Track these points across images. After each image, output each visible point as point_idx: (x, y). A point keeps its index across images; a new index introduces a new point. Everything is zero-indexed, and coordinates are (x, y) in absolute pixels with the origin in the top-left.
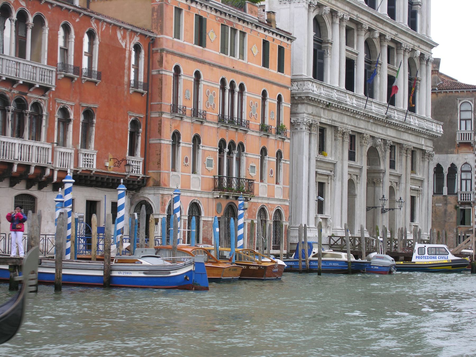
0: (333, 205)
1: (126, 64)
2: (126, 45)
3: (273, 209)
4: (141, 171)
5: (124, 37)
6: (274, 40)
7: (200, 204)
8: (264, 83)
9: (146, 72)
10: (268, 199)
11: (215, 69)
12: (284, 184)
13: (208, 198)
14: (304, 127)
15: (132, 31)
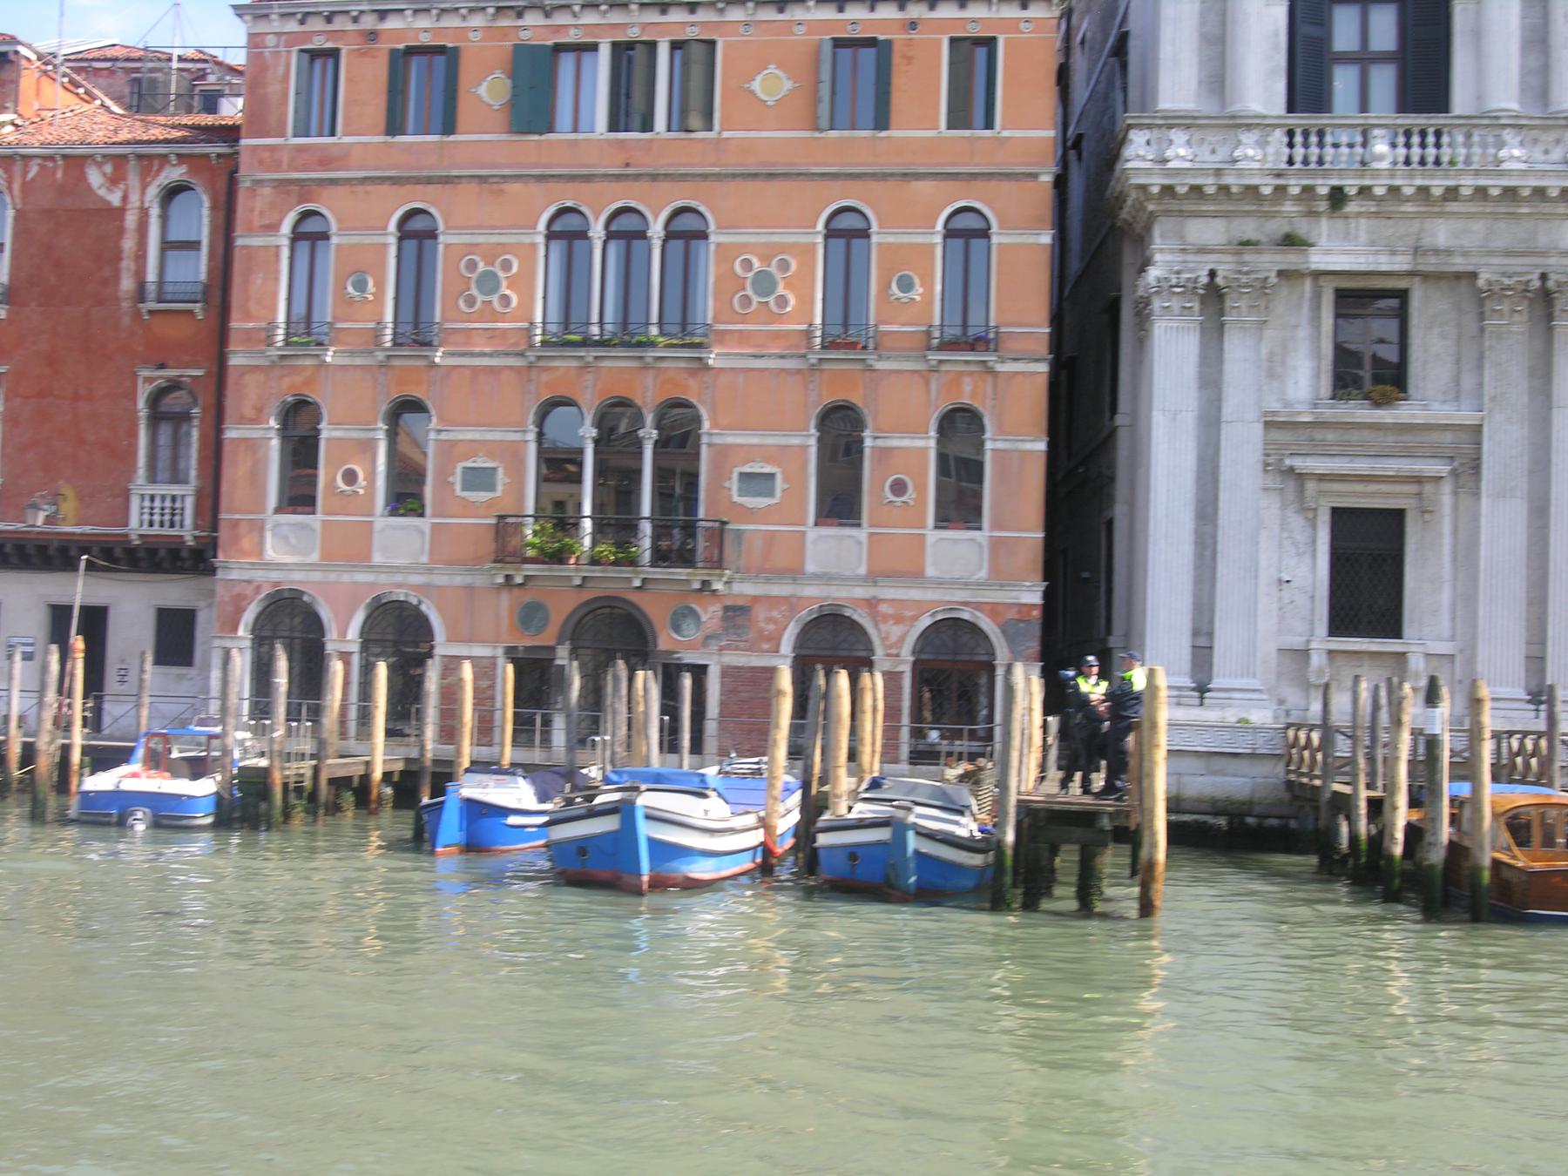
0: (1467, 600)
1: (128, 244)
2: (125, 198)
3: (915, 618)
4: (188, 521)
5: (114, 180)
6: (913, 25)
7: (423, 608)
8: (837, 185)
9: (220, 250)
10: (873, 577)
11: (516, 187)
12: (996, 525)
13: (470, 589)
14: (1157, 304)
15: (140, 157)
